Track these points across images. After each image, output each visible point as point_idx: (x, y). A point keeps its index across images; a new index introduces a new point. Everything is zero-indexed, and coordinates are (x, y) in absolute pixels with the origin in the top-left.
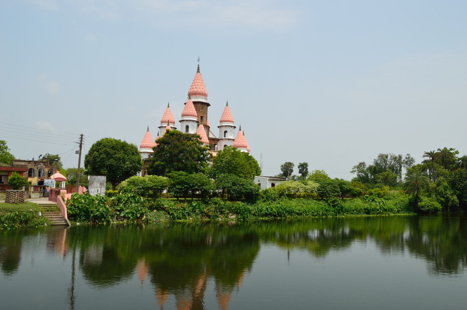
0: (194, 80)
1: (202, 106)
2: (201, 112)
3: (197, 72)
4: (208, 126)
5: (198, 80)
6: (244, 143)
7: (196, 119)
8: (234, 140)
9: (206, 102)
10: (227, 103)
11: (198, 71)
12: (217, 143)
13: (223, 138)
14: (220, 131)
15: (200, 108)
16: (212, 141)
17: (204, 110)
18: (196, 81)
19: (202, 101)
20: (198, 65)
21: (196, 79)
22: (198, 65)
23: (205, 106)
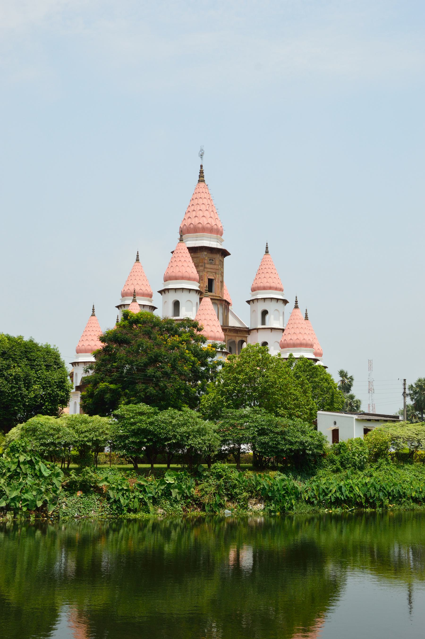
0: (193, 199)
1: (211, 256)
2: (209, 270)
3: (199, 181)
4: (226, 301)
5: (200, 198)
6: (306, 337)
7: (195, 286)
8: (283, 330)
9: (219, 247)
10: (267, 248)
11: (202, 179)
12: (247, 337)
13: (260, 326)
14: (253, 311)
15: (206, 261)
16: (235, 335)
17: (215, 264)
18: (196, 201)
19: (211, 246)
20: (201, 166)
21: (196, 196)
22: (201, 166)
23: (218, 257)
